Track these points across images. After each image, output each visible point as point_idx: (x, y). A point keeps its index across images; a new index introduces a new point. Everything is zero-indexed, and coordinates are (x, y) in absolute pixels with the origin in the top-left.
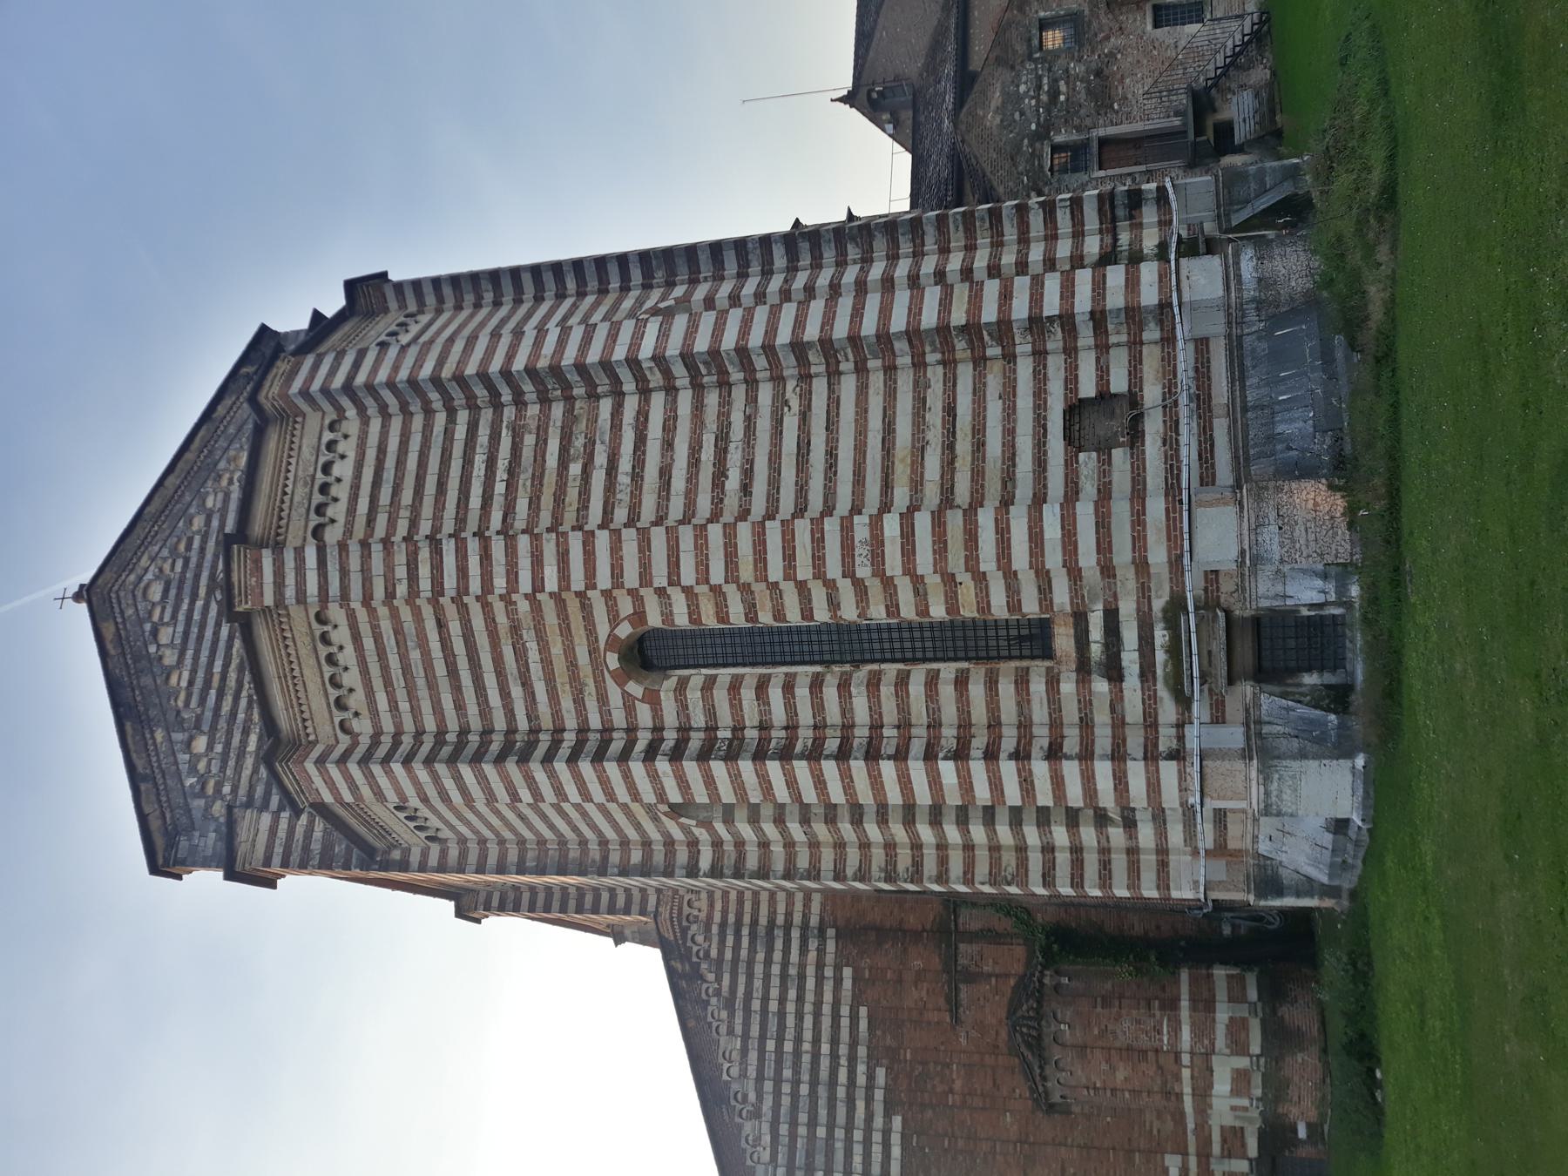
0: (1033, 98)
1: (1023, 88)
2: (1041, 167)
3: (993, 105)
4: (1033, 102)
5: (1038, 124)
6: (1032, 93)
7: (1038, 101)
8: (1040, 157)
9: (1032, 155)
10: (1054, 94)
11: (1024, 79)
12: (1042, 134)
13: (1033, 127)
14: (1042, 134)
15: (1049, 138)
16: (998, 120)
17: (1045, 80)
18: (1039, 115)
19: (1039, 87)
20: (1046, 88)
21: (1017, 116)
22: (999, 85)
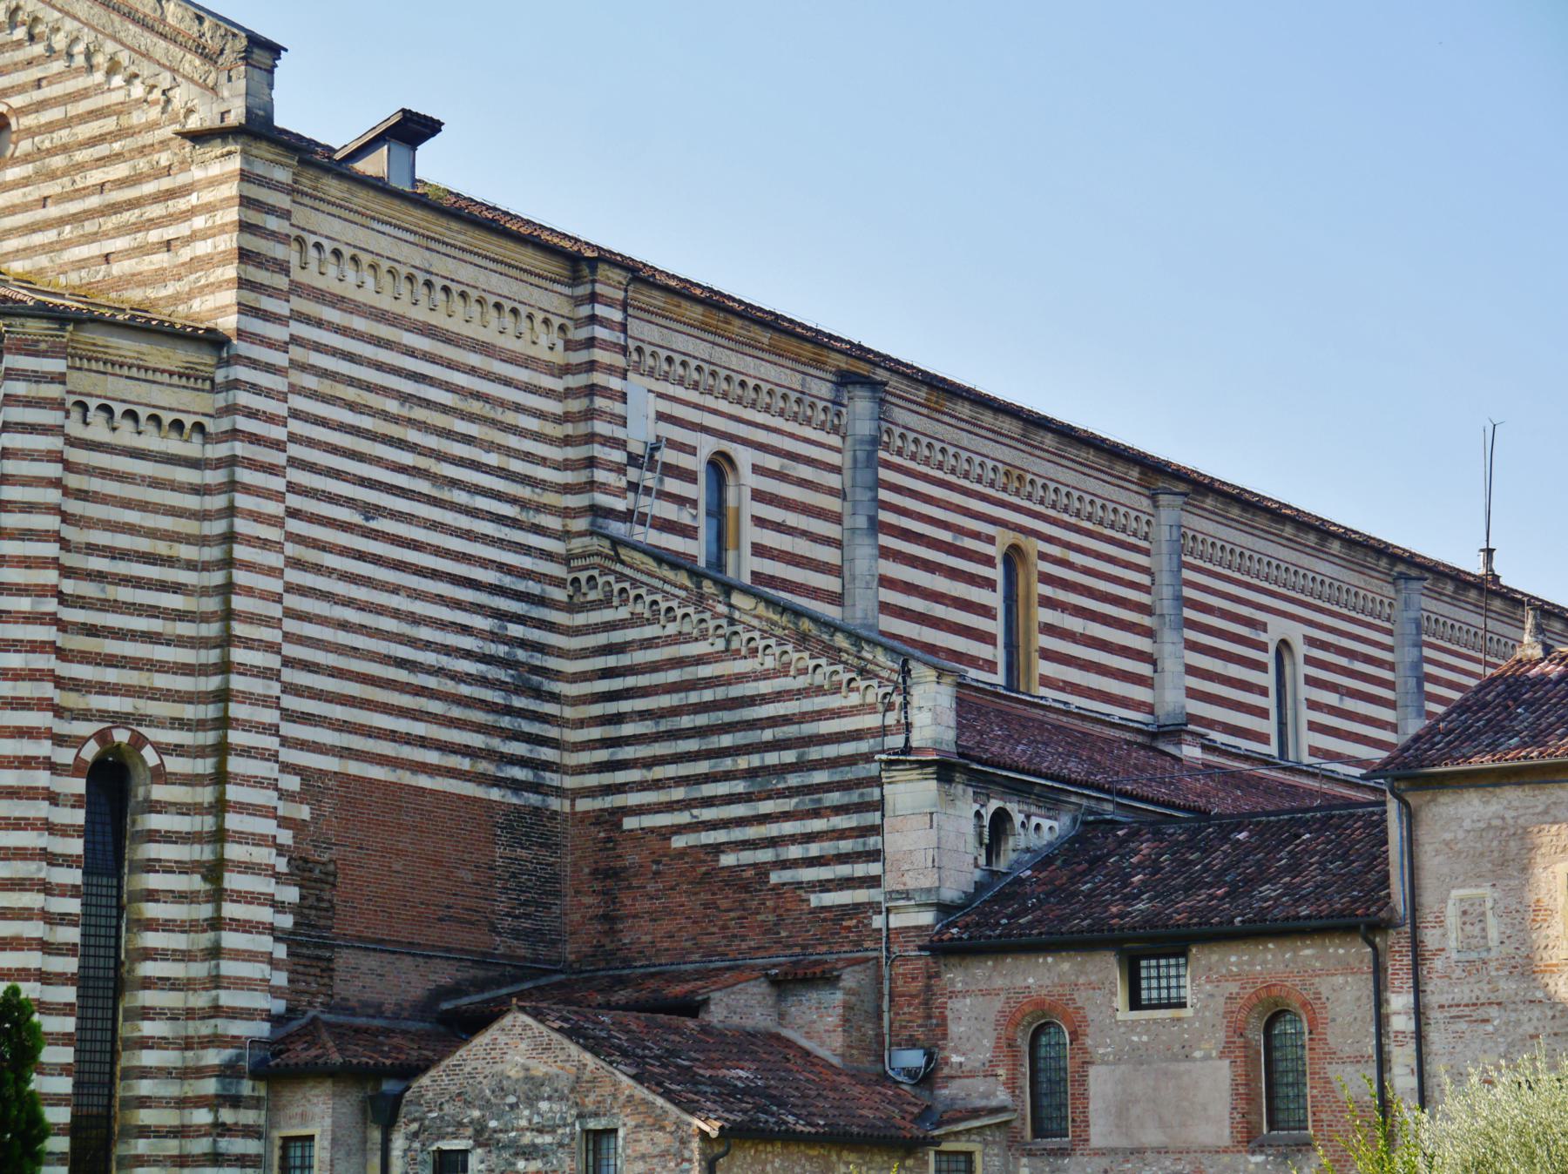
0: (530, 1121)
1: (544, 1106)
2: (442, 1137)
3: (531, 1063)
4: (524, 1123)
5: (495, 1131)
6: (536, 1119)
7: (523, 1129)
8: (455, 1136)
9: (460, 1124)
10: (530, 1152)
11: (556, 1107)
12: (482, 1137)
13: (493, 1124)
14: (482, 1137)
15: (474, 1148)
16: (512, 1073)
17: (548, 1139)
18: (506, 1131)
19: (540, 1131)
20: (539, 1141)
21: (512, 1099)
22: (554, 1070)
